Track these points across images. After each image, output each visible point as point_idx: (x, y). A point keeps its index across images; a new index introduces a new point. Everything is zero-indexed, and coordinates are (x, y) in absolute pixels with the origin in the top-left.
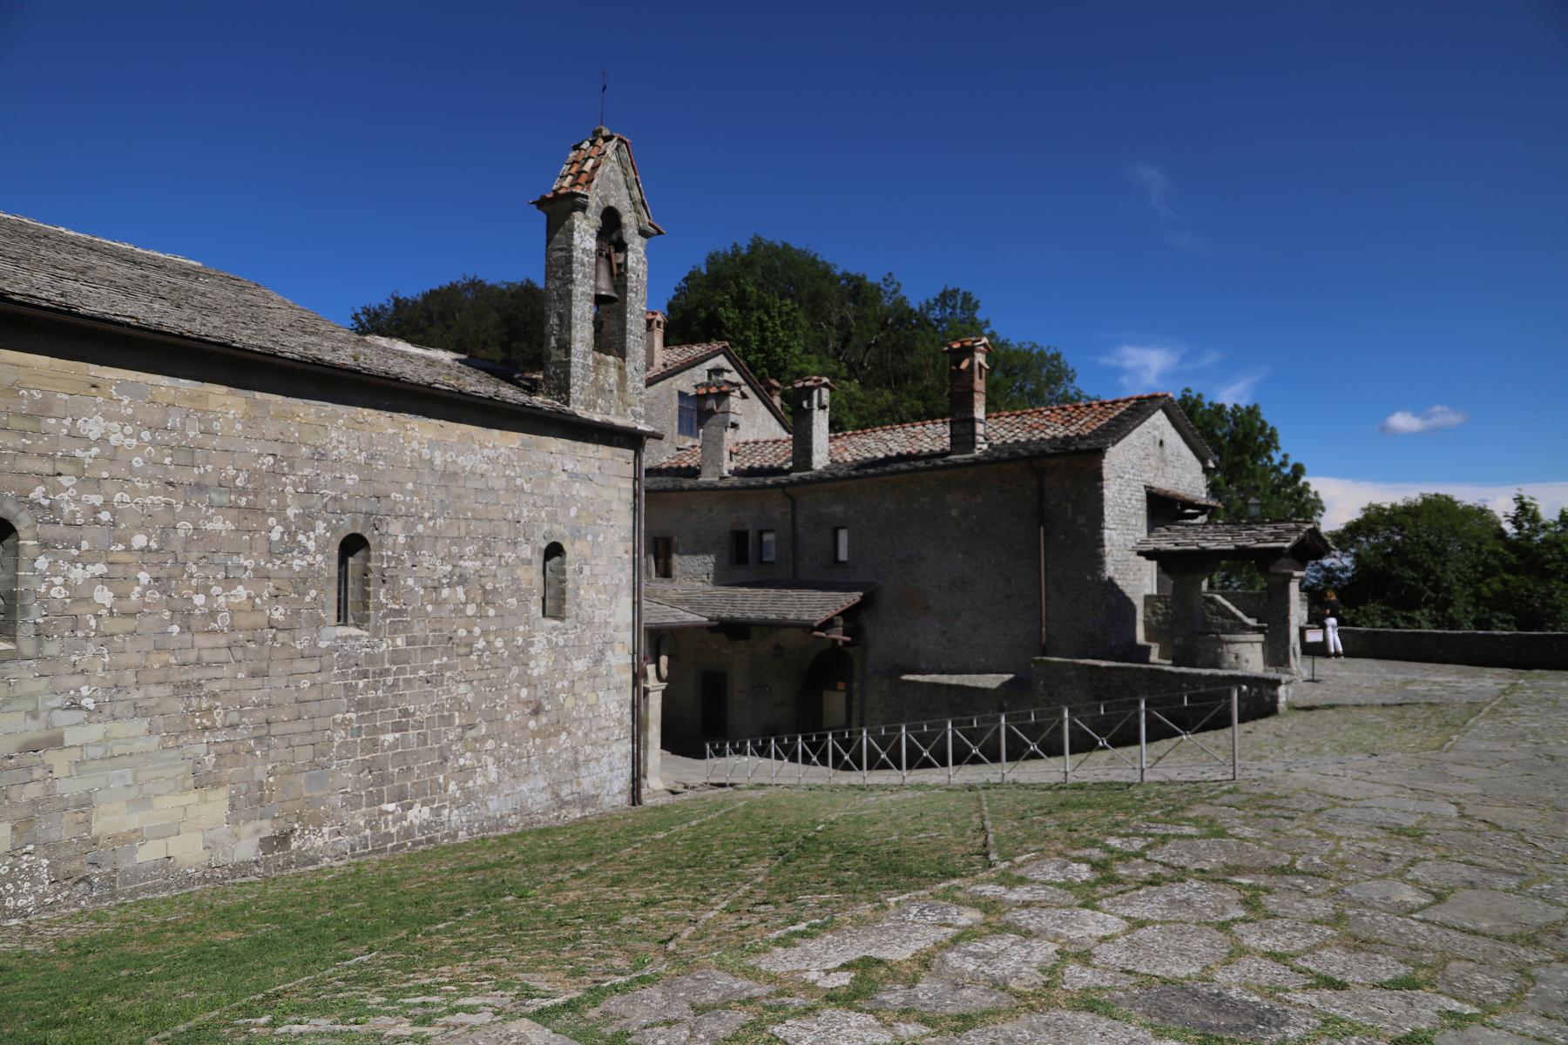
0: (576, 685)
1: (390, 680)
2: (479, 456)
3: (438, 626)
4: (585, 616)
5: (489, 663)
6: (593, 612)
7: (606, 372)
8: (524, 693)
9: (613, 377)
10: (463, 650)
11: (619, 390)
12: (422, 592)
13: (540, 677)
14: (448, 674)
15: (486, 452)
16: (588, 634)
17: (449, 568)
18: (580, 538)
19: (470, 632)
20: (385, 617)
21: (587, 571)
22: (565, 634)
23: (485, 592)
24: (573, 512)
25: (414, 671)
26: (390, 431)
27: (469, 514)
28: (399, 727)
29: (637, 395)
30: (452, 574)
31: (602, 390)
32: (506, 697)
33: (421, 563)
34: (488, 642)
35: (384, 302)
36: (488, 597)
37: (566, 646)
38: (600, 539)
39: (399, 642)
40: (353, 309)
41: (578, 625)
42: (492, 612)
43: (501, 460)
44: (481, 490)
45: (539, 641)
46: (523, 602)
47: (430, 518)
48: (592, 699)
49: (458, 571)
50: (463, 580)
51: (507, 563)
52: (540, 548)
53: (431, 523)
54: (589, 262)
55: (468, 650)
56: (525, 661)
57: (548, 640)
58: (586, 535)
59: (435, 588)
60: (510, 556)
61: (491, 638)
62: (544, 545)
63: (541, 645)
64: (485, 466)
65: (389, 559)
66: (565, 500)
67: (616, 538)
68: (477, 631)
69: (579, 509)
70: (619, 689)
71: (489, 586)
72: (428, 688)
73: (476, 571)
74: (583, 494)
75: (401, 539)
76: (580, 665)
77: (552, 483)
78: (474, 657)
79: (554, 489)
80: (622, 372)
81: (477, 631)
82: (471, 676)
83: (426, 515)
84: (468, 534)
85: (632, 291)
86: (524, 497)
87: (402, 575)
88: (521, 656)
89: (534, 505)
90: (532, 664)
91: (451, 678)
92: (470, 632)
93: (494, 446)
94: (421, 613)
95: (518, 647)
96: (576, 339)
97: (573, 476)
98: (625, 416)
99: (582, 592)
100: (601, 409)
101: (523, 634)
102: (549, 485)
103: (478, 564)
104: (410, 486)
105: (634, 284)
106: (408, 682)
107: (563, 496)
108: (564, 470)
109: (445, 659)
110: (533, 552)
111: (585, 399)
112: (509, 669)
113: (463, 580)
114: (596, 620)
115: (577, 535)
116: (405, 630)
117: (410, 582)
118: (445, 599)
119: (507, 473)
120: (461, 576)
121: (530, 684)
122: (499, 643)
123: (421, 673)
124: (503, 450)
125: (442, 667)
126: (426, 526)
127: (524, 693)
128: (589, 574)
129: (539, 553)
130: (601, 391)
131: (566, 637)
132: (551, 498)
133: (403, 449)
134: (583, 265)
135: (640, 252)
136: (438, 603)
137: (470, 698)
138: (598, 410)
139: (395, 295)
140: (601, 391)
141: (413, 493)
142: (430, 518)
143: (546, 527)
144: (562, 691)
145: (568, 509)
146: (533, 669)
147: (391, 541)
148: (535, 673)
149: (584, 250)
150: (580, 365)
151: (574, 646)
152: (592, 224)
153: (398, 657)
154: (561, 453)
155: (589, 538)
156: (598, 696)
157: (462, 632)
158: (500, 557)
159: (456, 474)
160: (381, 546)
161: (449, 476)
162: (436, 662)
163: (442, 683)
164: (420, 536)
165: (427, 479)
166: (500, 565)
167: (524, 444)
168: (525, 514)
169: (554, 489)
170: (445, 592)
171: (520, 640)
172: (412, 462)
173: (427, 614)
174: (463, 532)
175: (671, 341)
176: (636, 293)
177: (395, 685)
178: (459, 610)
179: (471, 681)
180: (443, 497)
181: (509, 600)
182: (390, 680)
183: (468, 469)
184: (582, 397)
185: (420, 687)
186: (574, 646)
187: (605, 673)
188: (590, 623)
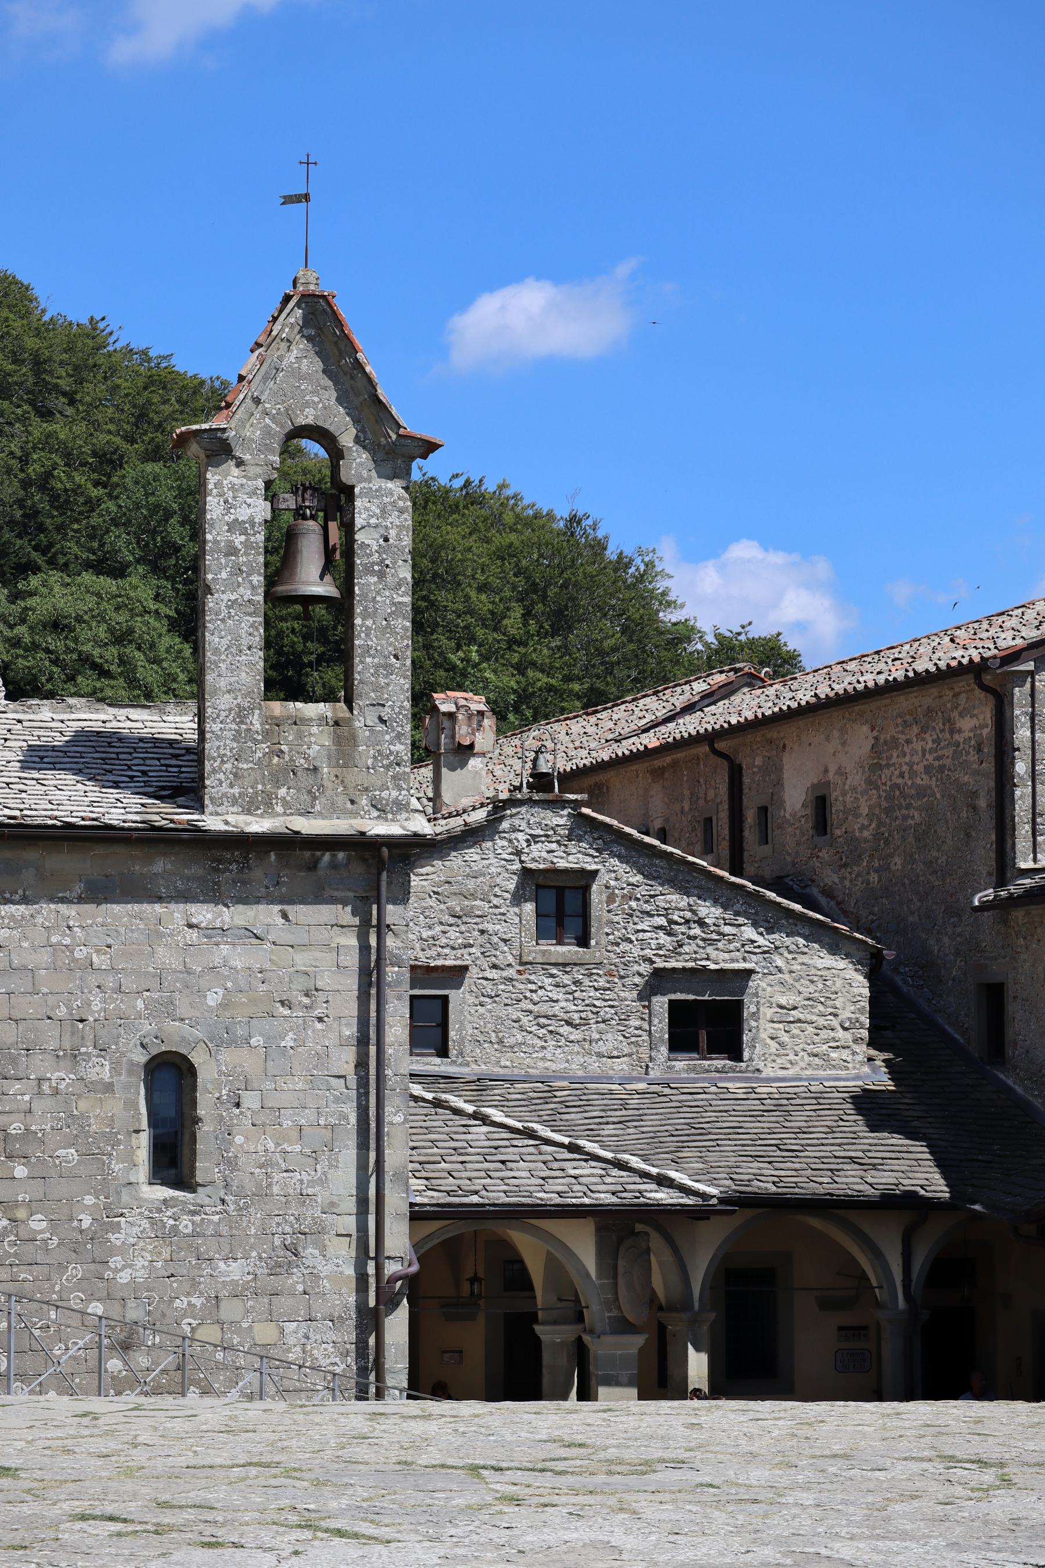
0: (223, 1305)
4: (247, 1181)
5: (16, 1255)
7: (300, 736)
8: (97, 1308)
13: (133, 1284)
21: (251, 1100)
22: (194, 1213)
24: (213, 999)
29: (387, 767)
37: (194, 1235)
38: (288, 1041)
42: (20, 1171)
51: (56, 1092)
52: (132, 1064)
54: (247, 544)
56: (98, 1254)
60: (61, 1076)
61: (21, 1214)
62: (141, 1058)
63: (136, 1230)
67: (331, 1039)
74: (238, 964)
76: (235, 1271)
77: (160, 951)
85: (368, 570)
86: (93, 980)
90: (116, 1261)
95: (81, 1232)
96: (215, 691)
98: (355, 814)
99: (239, 1139)
100: (286, 804)
101: (91, 1210)
107: (188, 972)
108: (190, 926)
110: (115, 1070)
112: (62, 1267)
114: (276, 1189)
119: (54, 939)
121: (109, 1297)
122: (38, 1224)
127: (97, 1308)
128: (256, 1106)
129: (130, 1073)
131: (197, 1218)
138: (279, 809)
143: (147, 1027)
145: (201, 994)
146: (117, 1271)
148: (124, 1277)
149: (234, 526)
150: (229, 734)
155: (257, 1040)
156: (282, 1331)
158: (40, 1080)
166: (40, 1093)
168: (97, 1005)
176: (381, 575)
181: (60, 1152)
184: (236, 790)
187: (300, 1288)
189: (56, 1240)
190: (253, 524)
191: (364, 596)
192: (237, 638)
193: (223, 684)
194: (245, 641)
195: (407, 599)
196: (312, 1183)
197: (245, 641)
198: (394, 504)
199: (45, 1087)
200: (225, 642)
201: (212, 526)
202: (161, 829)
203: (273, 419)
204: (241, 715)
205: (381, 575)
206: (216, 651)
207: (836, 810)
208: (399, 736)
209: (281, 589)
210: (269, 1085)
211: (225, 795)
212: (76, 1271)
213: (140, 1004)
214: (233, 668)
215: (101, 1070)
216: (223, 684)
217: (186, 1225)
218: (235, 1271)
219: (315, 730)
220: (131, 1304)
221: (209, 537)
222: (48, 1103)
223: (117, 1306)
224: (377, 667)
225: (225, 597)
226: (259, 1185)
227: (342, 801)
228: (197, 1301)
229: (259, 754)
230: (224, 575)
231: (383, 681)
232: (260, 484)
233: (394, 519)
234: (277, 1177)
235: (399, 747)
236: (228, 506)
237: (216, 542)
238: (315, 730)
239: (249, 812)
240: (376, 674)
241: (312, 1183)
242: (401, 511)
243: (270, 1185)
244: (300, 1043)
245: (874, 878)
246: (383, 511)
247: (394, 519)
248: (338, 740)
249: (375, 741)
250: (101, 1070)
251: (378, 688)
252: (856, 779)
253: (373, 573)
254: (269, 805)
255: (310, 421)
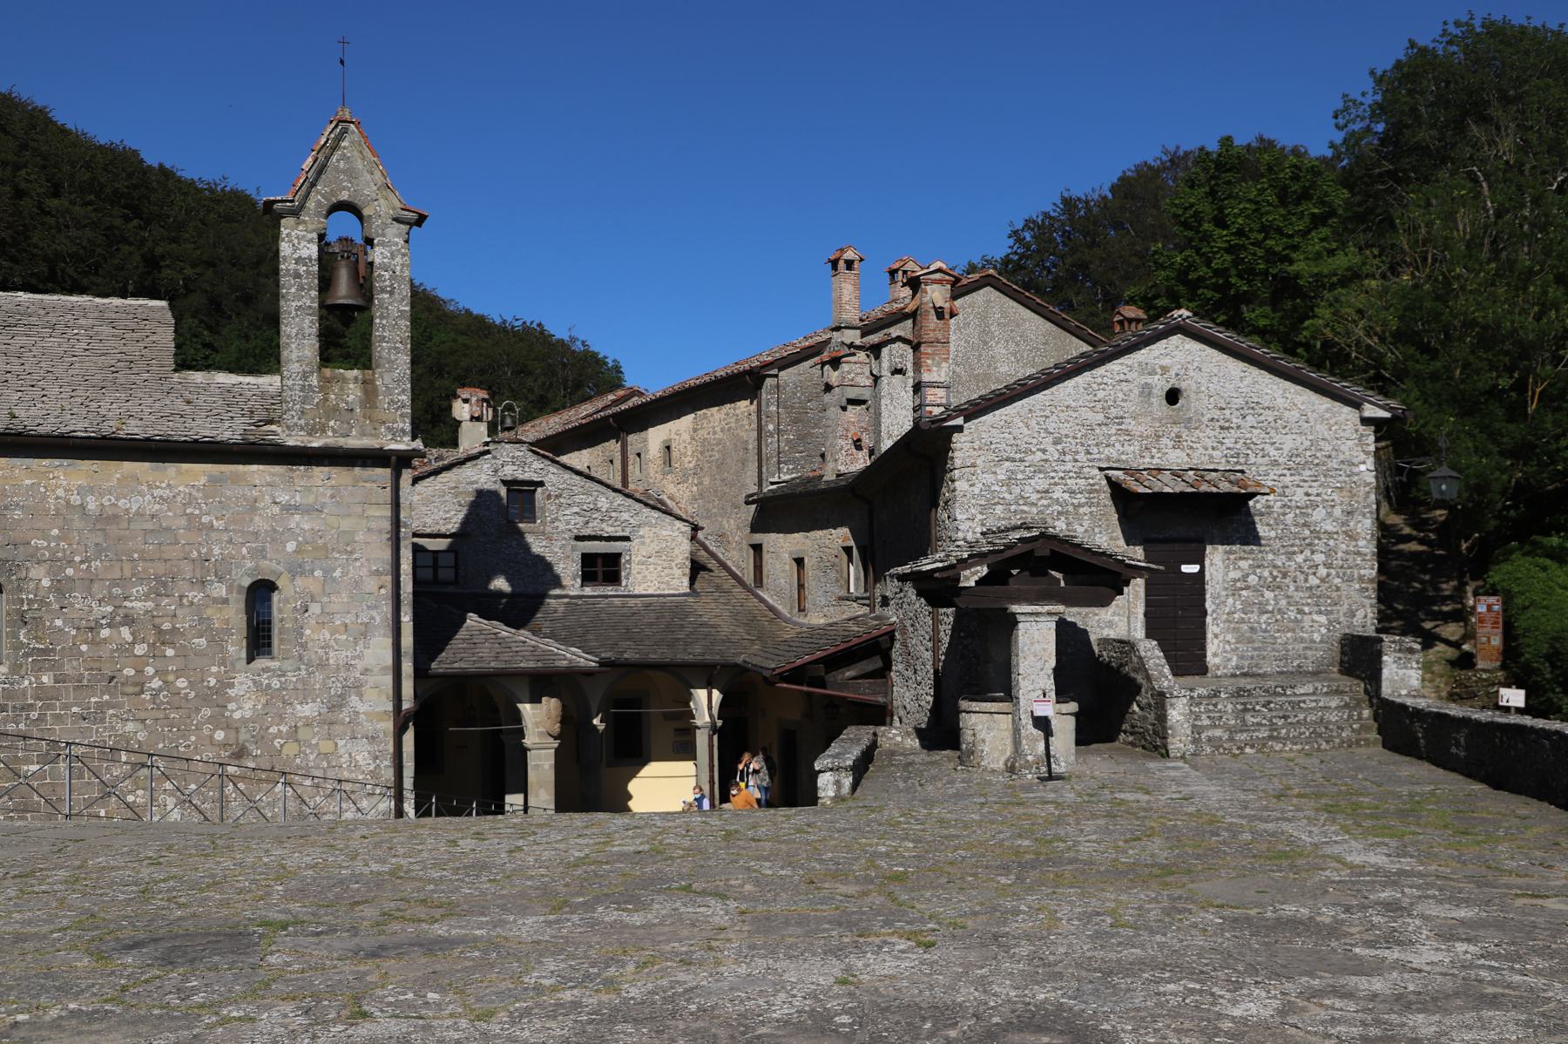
0: (300, 731)
1: (34, 715)
2: (148, 497)
3: (97, 665)
5: (167, 703)
6: (327, 653)
7: (342, 389)
8: (220, 735)
9: (353, 393)
10: (130, 689)
11: (363, 406)
12: (74, 632)
13: (244, 721)
14: (111, 711)
15: (157, 492)
16: (319, 676)
17: (110, 609)
18: (302, 573)
19: (139, 672)
20: (27, 655)
21: (315, 608)
22: (279, 676)
23: (160, 632)
24: (291, 546)
25: (66, 707)
26: (28, 482)
27: (136, 556)
28: (43, 759)
29: (397, 409)
30: (112, 615)
31: (336, 409)
32: (193, 738)
33: (72, 605)
34: (165, 682)
35: (1049, 208)
36: (164, 638)
38: (337, 574)
39: (45, 679)
40: (1011, 224)
41: (303, 667)
42: (170, 652)
43: (179, 499)
44: (152, 531)
45: (242, 683)
46: (217, 640)
47: (82, 562)
48: (326, 746)
49: (121, 612)
50: (129, 620)
51: (192, 603)
53: (84, 566)
54: (307, 272)
55: (137, 689)
56: (220, 702)
57: (255, 682)
58: (312, 571)
59: (91, 629)
60: (195, 595)
61: (171, 678)
62: (247, 582)
63: (245, 686)
64: (157, 507)
65: (30, 602)
66: (277, 537)
68: (150, 670)
69: (299, 544)
70: (372, 739)
71: (166, 626)
72: (85, 724)
73: (147, 612)
74: (306, 527)
75: (46, 583)
76: (307, 710)
78: (147, 696)
79: (260, 523)
80: (370, 387)
81: (150, 670)
82: (142, 715)
83: (77, 559)
84: (133, 575)
85: (383, 290)
86: (214, 535)
87: (46, 617)
88: (217, 697)
89: (230, 541)
91: (114, 715)
92: (139, 672)
93: (169, 485)
94: (74, 652)
95: (209, 688)
97: (289, 509)
98: (376, 436)
99: (308, 632)
100: (334, 431)
101: (217, 675)
102: (251, 520)
103: (150, 605)
104: (55, 532)
105: (388, 283)
106: (58, 718)
107: (274, 530)
108: (276, 503)
109: (106, 697)
110: (229, 590)
111: (306, 424)
112: (198, 710)
113: (129, 620)
114: (331, 661)
115: (296, 570)
116: (52, 668)
117: (59, 623)
118: (105, 639)
119: (188, 511)
120: (126, 616)
121: (228, 727)
123: (75, 709)
124: (181, 488)
125: (101, 707)
126: (77, 569)
127: (220, 735)
128: (318, 611)
129: (239, 592)
130: (333, 412)
132: (256, 534)
133: (45, 497)
134: (297, 275)
135: (397, 244)
136: (93, 643)
137: (141, 736)
138: (330, 434)
139: (1066, 195)
140: (333, 412)
141: (58, 539)
142: (82, 562)
143: (249, 564)
144: (279, 734)
146: (233, 711)
147: (32, 585)
148: (237, 715)
149: (299, 260)
150: (297, 387)
151: (296, 689)
152: (310, 227)
153: (40, 692)
154: (269, 485)
155: (318, 573)
156: (336, 745)
157: (129, 672)
158: (181, 597)
159: (115, 516)
160: (20, 589)
161: (106, 519)
162: (93, 700)
163: (103, 720)
164: (69, 578)
165: (78, 523)
166: (181, 605)
167: (213, 480)
168: (217, 551)
169: (260, 523)
170: (105, 633)
171: (213, 682)
172: (57, 509)
173: (81, 654)
174: (127, 573)
175: (333, 352)
176: (391, 293)
177: (41, 719)
178: (125, 649)
179: (143, 721)
180: (99, 540)
181: (195, 640)
182: (34, 715)
183: (134, 509)
184: (302, 422)
185: (73, 723)
186: (296, 689)
187: (348, 719)
188: (323, 665)
189: (193, 694)
190: (311, 260)
191: (381, 306)
192: (302, 329)
193: (294, 356)
194: (307, 331)
195: (407, 308)
196: (354, 658)
197: (307, 331)
198: (399, 250)
199: (185, 601)
200: (294, 331)
201: (285, 260)
202: (253, 444)
203: (323, 197)
204: (305, 376)
205: (391, 293)
206: (289, 337)
207: (675, 454)
208: (404, 390)
209: (329, 302)
210: (325, 599)
211: (296, 424)
212: (207, 712)
213: (244, 551)
214: (300, 347)
215: (220, 590)
216: (294, 356)
217: (276, 684)
218: (307, 710)
219: (351, 386)
220: (243, 730)
221: (282, 267)
222: (186, 610)
223: (232, 734)
224: (390, 349)
225: (294, 304)
226: (321, 659)
227: (369, 429)
228: (284, 729)
229: (317, 400)
230: (293, 290)
231: (393, 357)
232: (315, 235)
233: (398, 260)
234: (332, 654)
235: (404, 397)
236: (295, 249)
237: (287, 270)
238: (351, 386)
239: (310, 435)
240: (389, 353)
241: (354, 658)
242: (404, 255)
243: (328, 659)
244: (344, 574)
245: (695, 489)
246: (392, 254)
247: (398, 260)
248: (366, 392)
249: (389, 391)
250: (220, 590)
251: (390, 362)
252: (686, 437)
253: (387, 292)
254: (324, 431)
255: (346, 198)
